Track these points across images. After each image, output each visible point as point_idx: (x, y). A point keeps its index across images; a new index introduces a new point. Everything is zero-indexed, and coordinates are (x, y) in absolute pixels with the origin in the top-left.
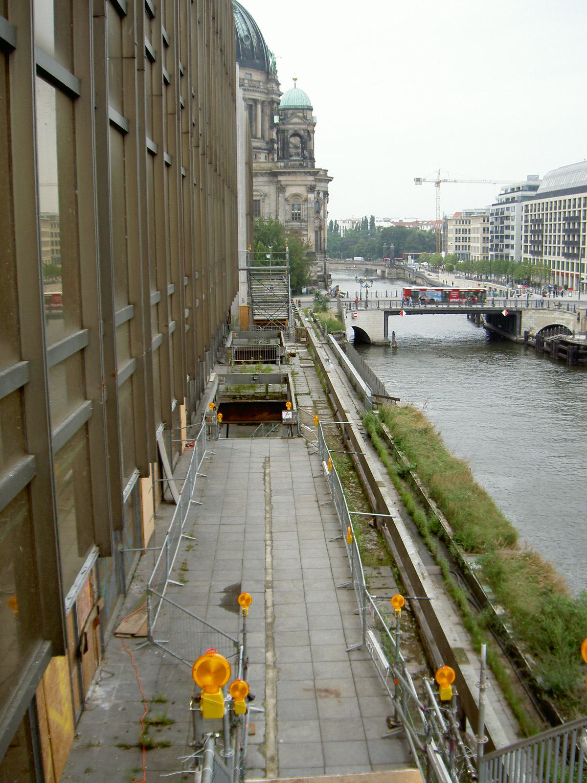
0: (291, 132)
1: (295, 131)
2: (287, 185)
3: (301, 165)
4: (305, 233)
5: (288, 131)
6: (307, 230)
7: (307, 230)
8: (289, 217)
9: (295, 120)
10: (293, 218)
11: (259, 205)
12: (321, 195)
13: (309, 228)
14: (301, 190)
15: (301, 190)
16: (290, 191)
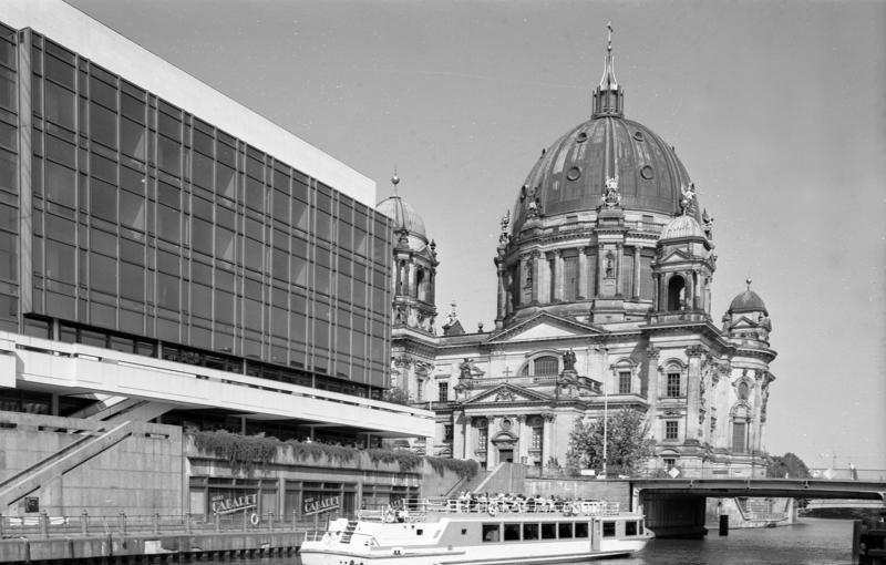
0: (669, 275)
1: (675, 273)
2: (661, 348)
3: (681, 319)
4: (683, 413)
5: (664, 273)
6: (686, 409)
7: (686, 409)
8: (662, 391)
9: (676, 258)
10: (669, 394)
11: (630, 379)
12: (751, 374)
13: (690, 407)
14: (680, 354)
15: (680, 354)
16: (664, 356)
